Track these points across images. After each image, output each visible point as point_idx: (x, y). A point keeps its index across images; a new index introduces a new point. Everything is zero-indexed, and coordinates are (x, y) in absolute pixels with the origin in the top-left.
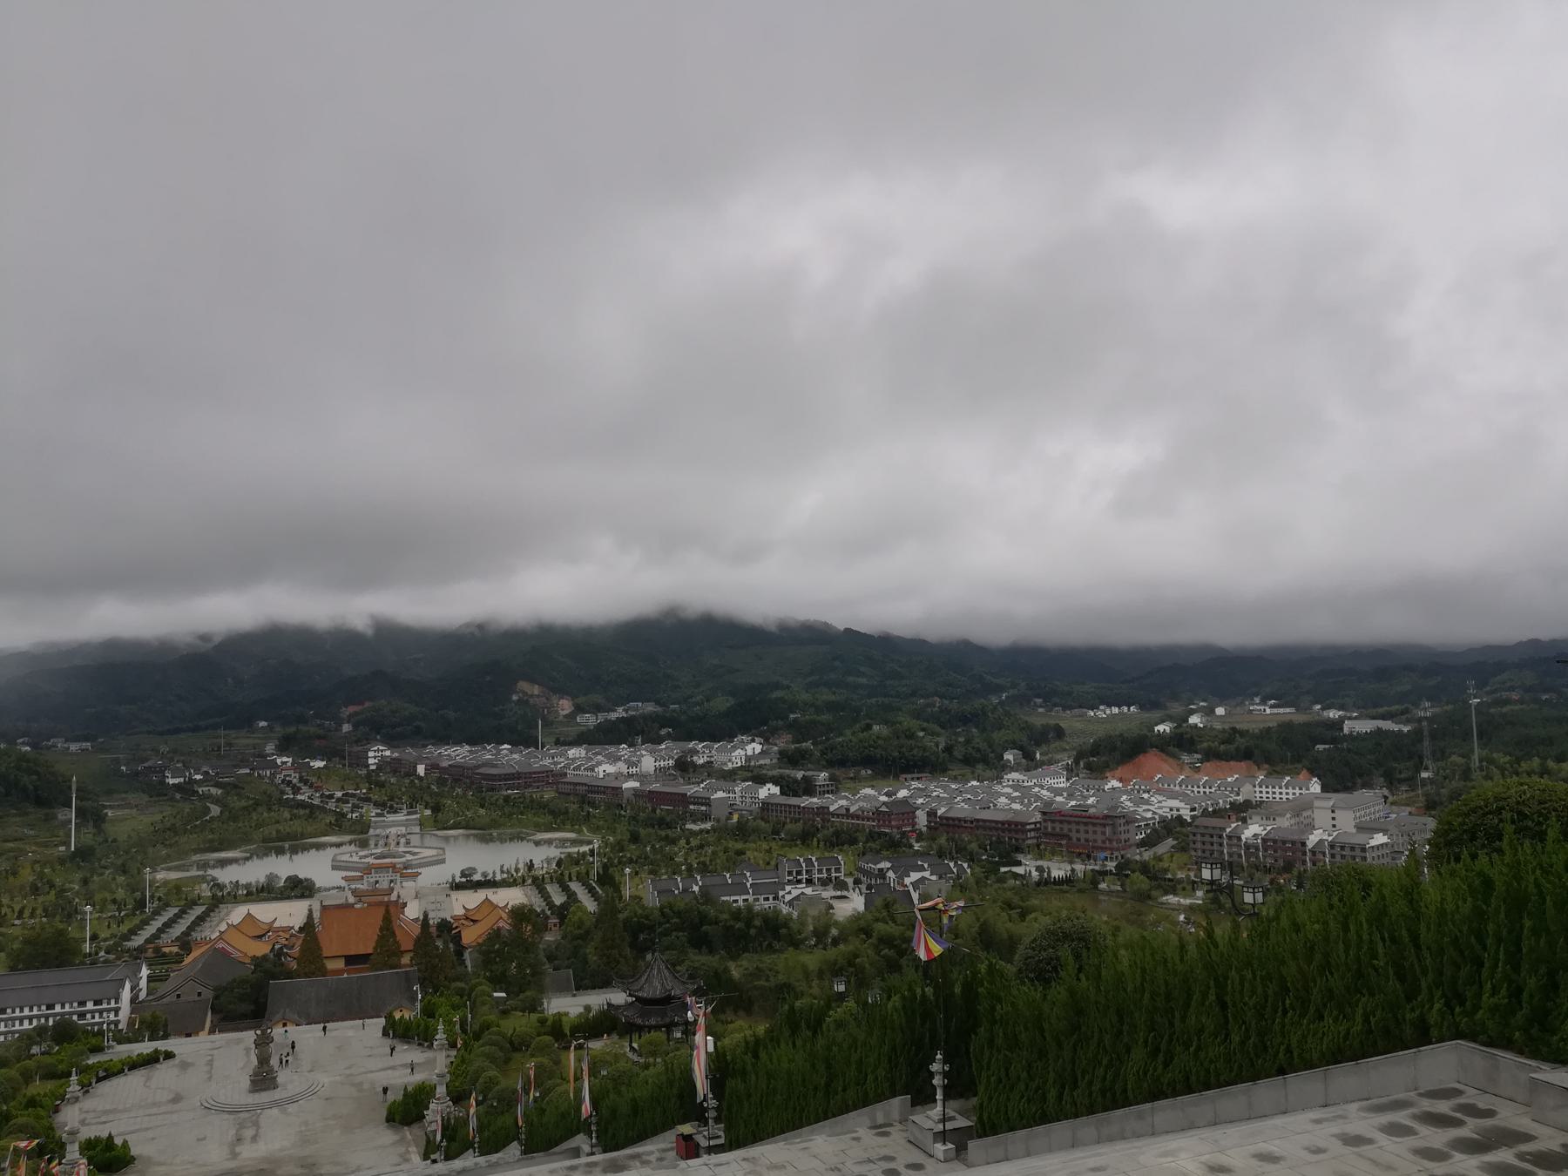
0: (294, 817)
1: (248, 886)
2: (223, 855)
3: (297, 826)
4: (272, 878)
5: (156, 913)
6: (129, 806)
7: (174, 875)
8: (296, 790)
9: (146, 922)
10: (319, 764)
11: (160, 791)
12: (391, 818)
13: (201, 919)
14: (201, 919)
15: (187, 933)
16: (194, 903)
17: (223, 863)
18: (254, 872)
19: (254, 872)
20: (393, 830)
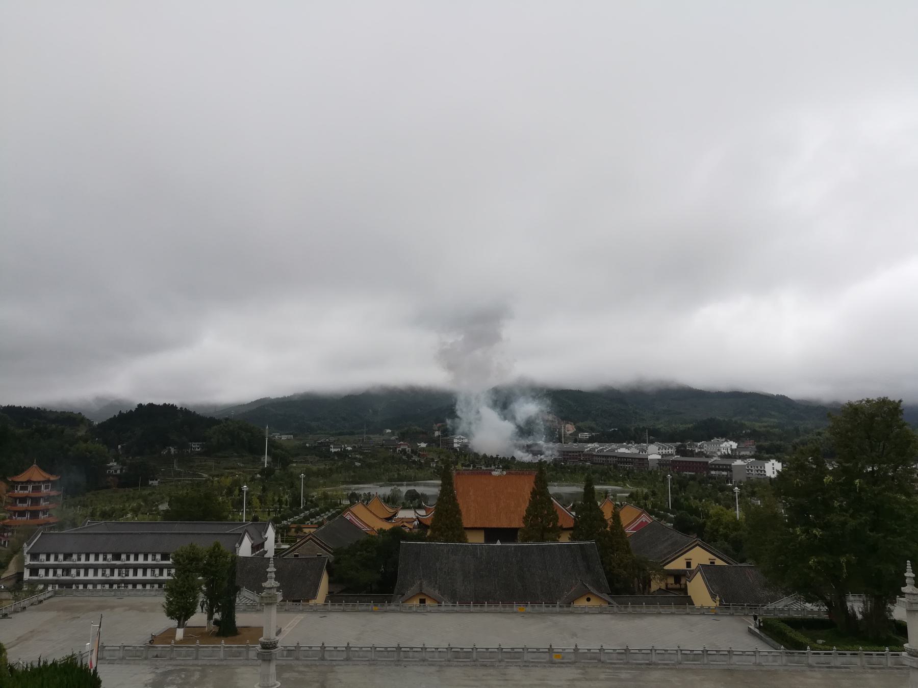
18: (386, 491)
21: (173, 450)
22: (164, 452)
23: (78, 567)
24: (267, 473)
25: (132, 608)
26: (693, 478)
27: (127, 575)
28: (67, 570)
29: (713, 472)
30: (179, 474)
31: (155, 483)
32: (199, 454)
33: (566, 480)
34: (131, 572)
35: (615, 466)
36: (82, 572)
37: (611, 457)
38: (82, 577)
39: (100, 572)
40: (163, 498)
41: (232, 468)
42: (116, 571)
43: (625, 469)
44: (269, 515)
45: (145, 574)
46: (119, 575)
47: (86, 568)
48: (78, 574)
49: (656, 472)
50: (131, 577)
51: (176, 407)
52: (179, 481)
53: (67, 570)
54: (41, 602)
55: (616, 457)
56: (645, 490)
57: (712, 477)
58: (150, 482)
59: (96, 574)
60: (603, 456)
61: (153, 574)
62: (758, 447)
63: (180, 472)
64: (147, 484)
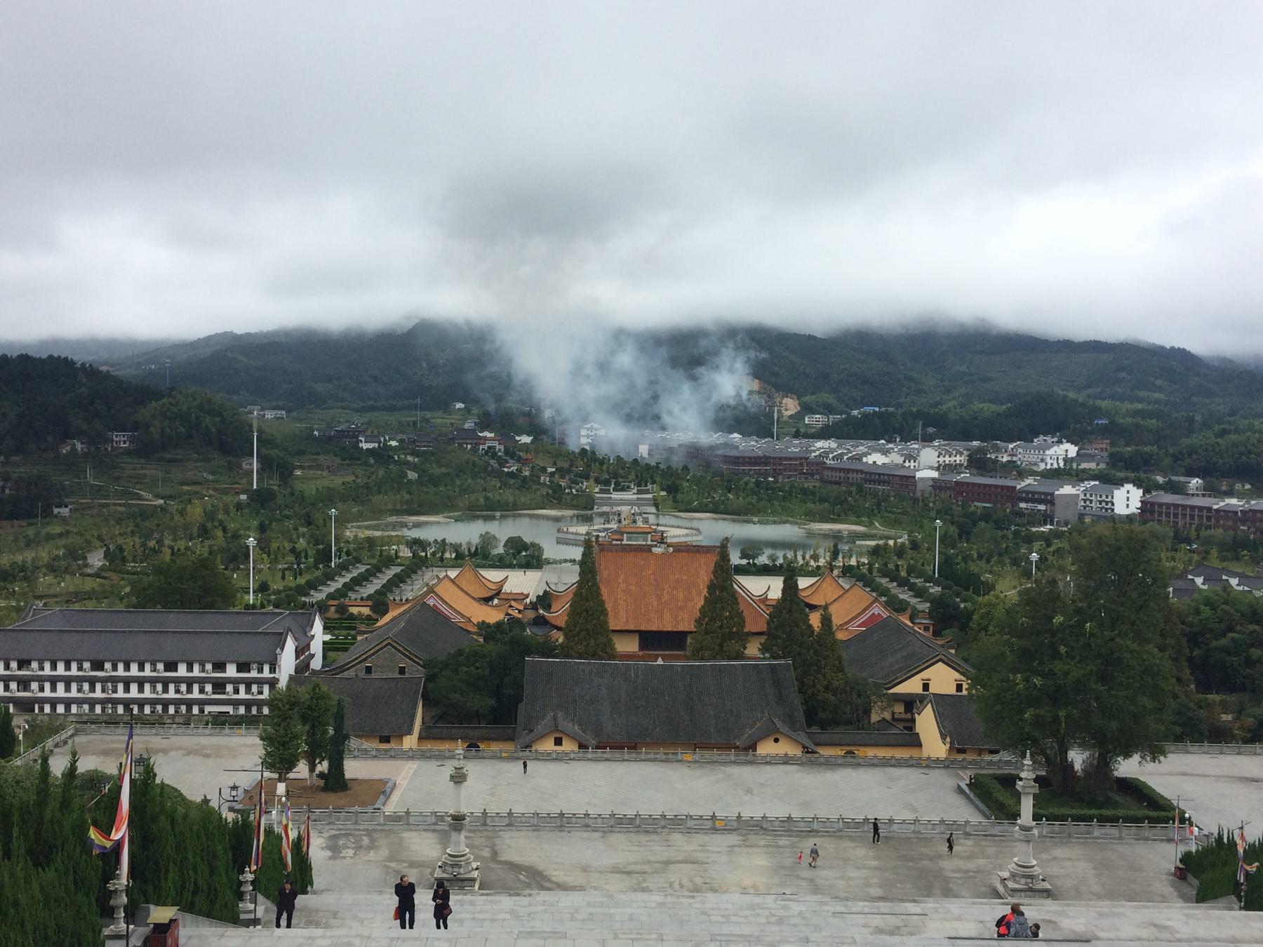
0: (505, 485)
1: (456, 548)
2: (423, 518)
3: (508, 495)
4: (488, 540)
5: (344, 567)
6: (319, 467)
7: (368, 533)
8: (502, 463)
9: (330, 577)
10: (526, 439)
11: (354, 456)
12: (616, 496)
13: (398, 580)
14: (398, 580)
15: (383, 592)
16: (390, 561)
17: (417, 525)
18: (466, 533)
19: (466, 533)
20: (625, 509)
21: (79, 446)
22: (65, 450)
23: (41, 680)
24: (262, 499)
25: (190, 752)
26: (986, 516)
27: (115, 691)
28: (24, 683)
29: (1023, 505)
30: (98, 492)
31: (65, 511)
32: (128, 453)
33: (774, 513)
34: (120, 687)
35: (860, 489)
36: (47, 686)
37: (853, 471)
38: (47, 693)
39: (74, 686)
40: (89, 542)
41: (195, 483)
42: (98, 686)
43: (875, 495)
44: (283, 578)
45: (141, 690)
46: (103, 691)
47: (54, 681)
48: (42, 689)
49: (925, 502)
50: (121, 694)
51: (72, 363)
52: (103, 506)
53: (24, 683)
54: (65, 742)
55: (862, 472)
56: (904, 539)
57: (1020, 514)
58: (56, 511)
59: (68, 689)
60: (840, 470)
61: (154, 690)
62: (1111, 456)
63: (100, 489)
64: (47, 513)
